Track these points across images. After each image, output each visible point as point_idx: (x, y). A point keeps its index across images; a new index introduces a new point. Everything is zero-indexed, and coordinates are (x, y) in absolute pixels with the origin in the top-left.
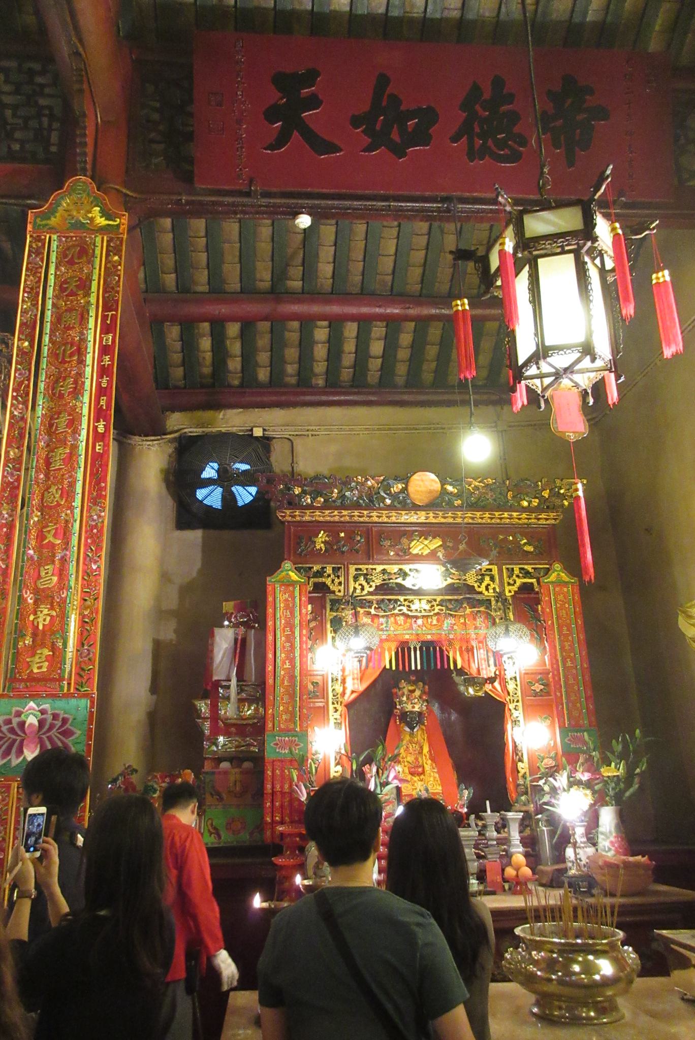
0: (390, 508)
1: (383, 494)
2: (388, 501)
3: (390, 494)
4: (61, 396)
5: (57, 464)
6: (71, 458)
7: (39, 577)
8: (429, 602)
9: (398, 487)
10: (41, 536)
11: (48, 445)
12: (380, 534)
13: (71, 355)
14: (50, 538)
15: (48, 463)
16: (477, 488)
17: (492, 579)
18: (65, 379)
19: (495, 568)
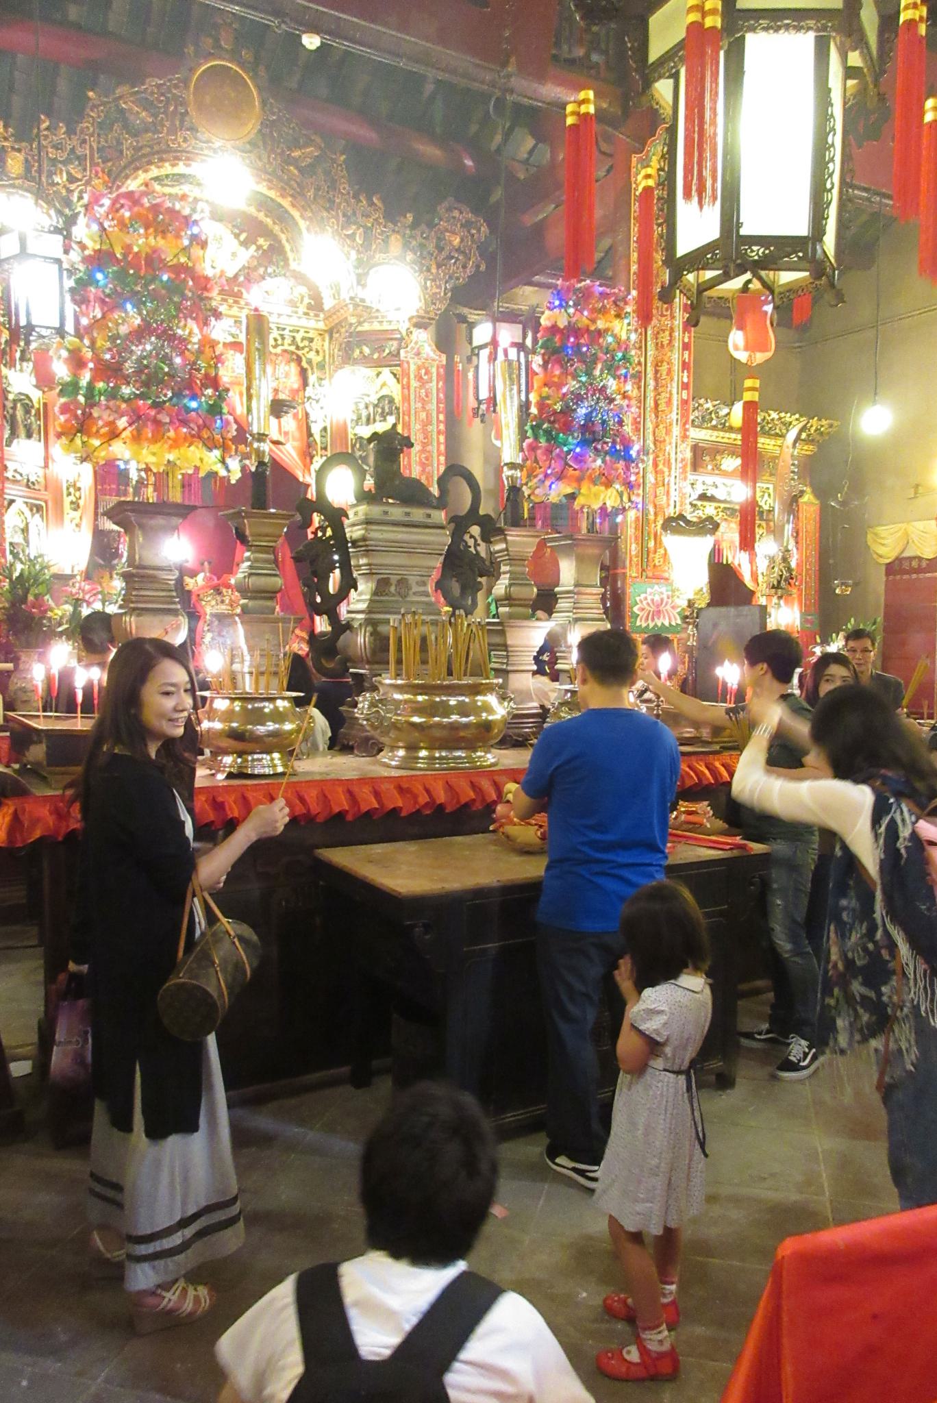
0: (714, 428)
1: (713, 416)
2: (714, 423)
3: (718, 417)
4: (662, 346)
5: (662, 407)
6: (669, 403)
7: (656, 496)
8: (716, 508)
9: (725, 411)
10: (655, 465)
11: (656, 389)
12: (704, 449)
13: (667, 310)
14: (661, 466)
15: (657, 405)
16: (773, 420)
17: (769, 495)
18: (664, 331)
19: (771, 486)
